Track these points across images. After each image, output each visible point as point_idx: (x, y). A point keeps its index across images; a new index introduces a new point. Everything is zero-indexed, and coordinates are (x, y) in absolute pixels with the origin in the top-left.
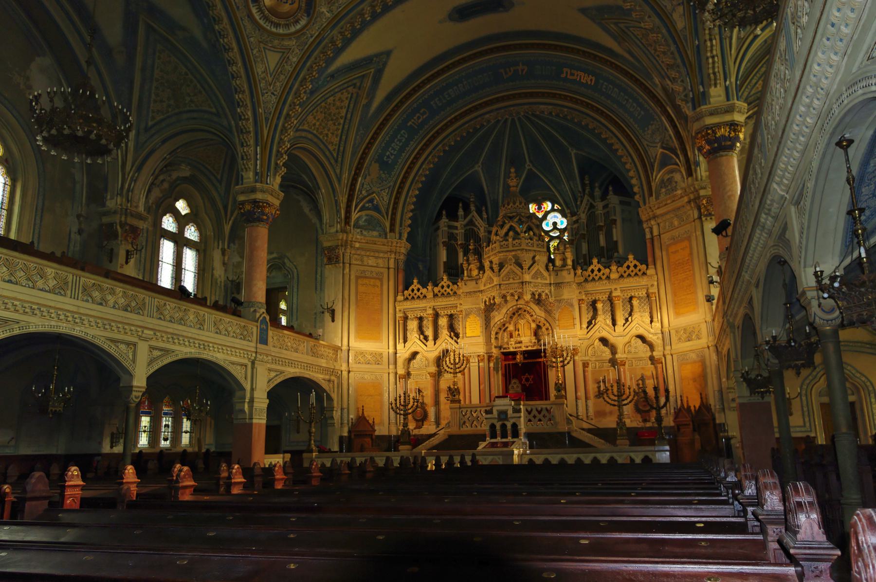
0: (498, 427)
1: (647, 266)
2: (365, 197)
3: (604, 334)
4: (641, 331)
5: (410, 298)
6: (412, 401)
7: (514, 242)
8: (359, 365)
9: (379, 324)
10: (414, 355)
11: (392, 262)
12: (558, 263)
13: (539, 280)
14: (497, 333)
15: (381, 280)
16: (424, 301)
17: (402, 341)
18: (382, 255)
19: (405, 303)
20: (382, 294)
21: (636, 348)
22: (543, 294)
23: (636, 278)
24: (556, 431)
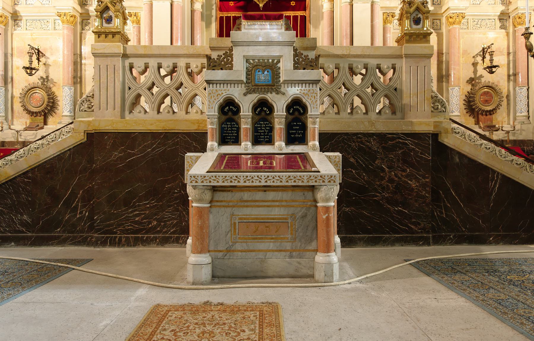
24: (406, 129)
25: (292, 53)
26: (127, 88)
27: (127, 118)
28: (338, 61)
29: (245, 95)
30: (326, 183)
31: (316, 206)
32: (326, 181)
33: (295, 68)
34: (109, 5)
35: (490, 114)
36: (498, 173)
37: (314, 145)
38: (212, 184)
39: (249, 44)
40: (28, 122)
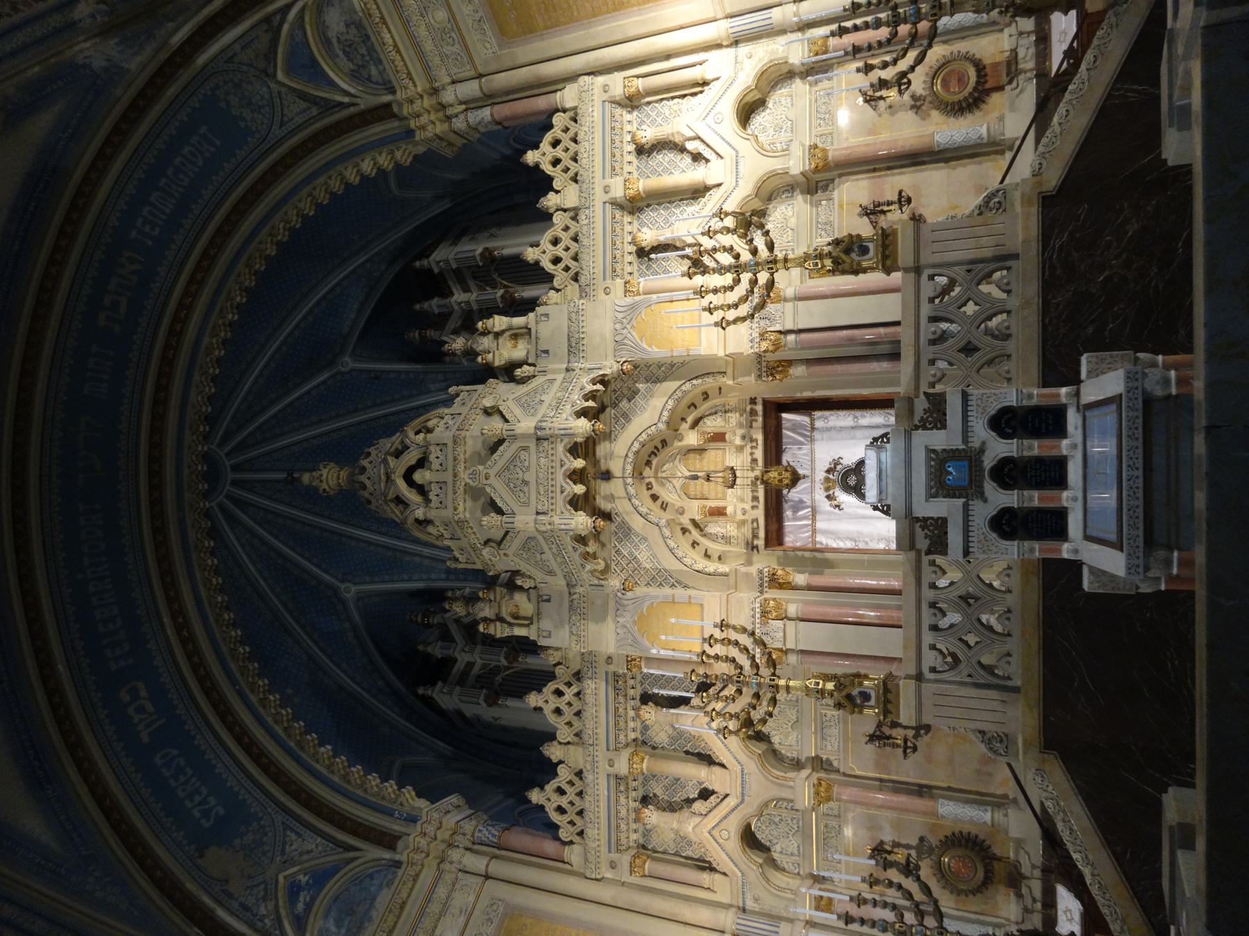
0: (1010, 499)
1: (557, 110)
2: (277, 906)
7: (435, 466)
14: (707, 556)
16: (589, 777)
17: (705, 878)
18: (441, 891)
22: (590, 387)
24: (1034, 249)
25: (920, 431)
26: (969, 680)
27: (1019, 683)
28: (924, 362)
29: (985, 501)
30: (1139, 384)
31: (1177, 396)
32: (1136, 384)
33: (944, 427)
34: (844, 693)
35: (984, 67)
36: (1112, 89)
37: (1068, 394)
38: (1141, 544)
40: (1002, 889)
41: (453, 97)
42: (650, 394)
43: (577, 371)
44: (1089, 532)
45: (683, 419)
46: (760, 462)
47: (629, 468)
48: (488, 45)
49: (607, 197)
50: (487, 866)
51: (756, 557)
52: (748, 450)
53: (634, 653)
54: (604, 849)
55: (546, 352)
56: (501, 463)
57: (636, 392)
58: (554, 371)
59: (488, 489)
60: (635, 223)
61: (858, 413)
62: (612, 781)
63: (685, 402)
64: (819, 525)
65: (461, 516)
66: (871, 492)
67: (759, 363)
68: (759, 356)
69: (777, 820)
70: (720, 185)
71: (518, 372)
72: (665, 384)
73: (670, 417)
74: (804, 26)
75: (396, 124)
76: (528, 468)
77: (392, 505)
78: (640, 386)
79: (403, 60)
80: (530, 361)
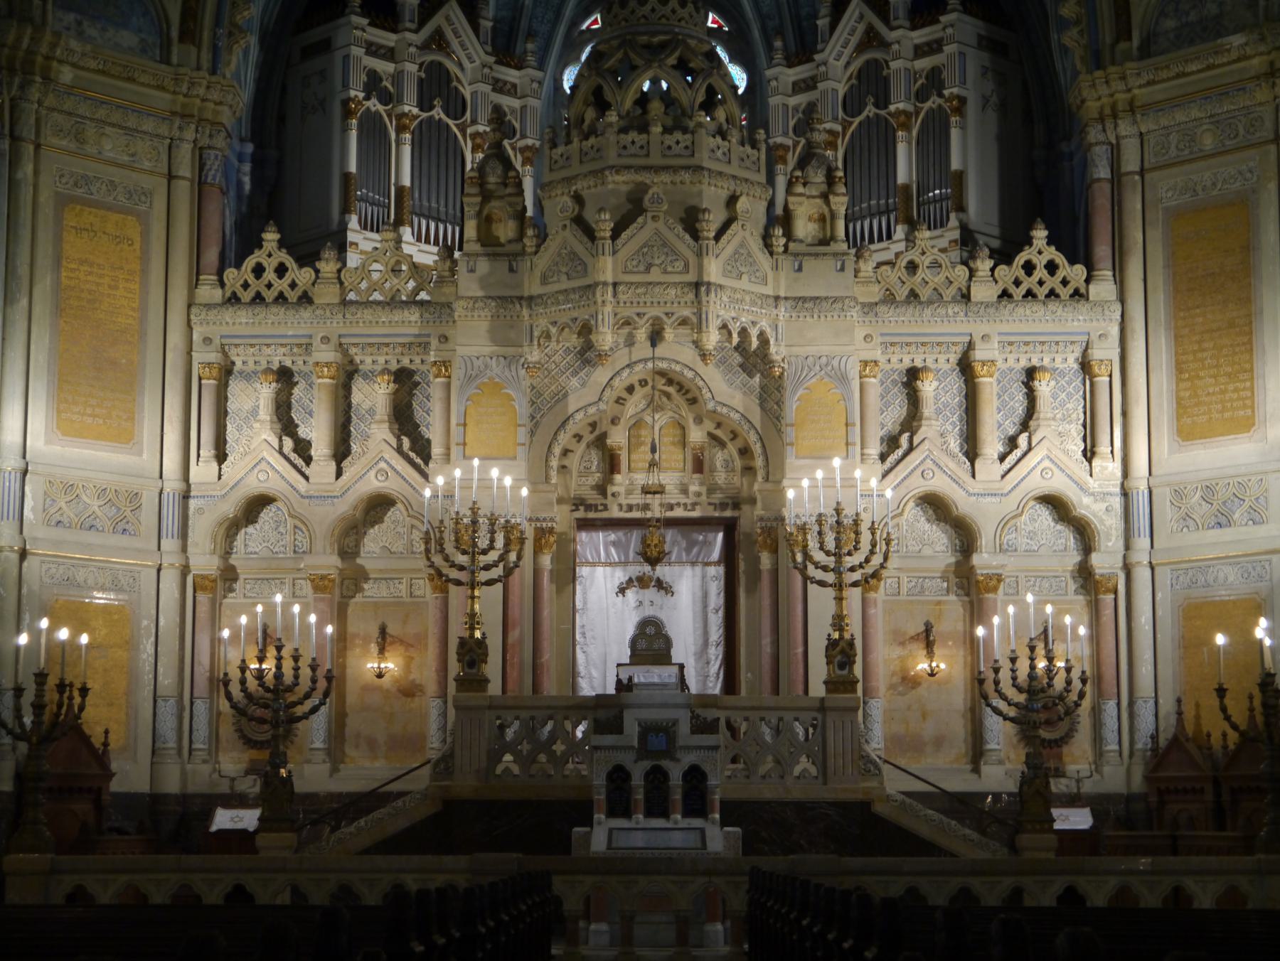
0: (637, 780)
1: (1090, 267)
3: (939, 484)
4: (1057, 484)
5: (246, 296)
6: (306, 672)
7: (669, 140)
8: (56, 533)
9: (129, 384)
10: (256, 505)
11: (185, 153)
12: (804, 228)
13: (744, 283)
14: (566, 452)
15: (144, 220)
16: (306, 313)
17: (208, 451)
18: (149, 125)
19: (228, 314)
20: (145, 272)
21: (1032, 535)
22: (754, 333)
23: (1053, 305)
33: (693, 732)
39: (640, 706)
41: (1124, 133)
42: (747, 391)
43: (775, 312)
44: (615, 832)
45: (719, 425)
46: (670, 514)
47: (663, 365)
48: (1170, 194)
49: (977, 339)
50: (184, 178)
51: (566, 508)
52: (683, 501)
53: (457, 373)
54: (225, 330)
55: (800, 269)
56: (670, 236)
57: (751, 375)
58: (776, 280)
59: (640, 220)
60: (949, 366)
61: (721, 613)
62: (304, 341)
63: (739, 429)
64: (600, 570)
65: (610, 178)
66: (642, 675)
67: (776, 519)
68: (783, 519)
69: (282, 529)
70: (974, 476)
71: (779, 231)
72: (758, 409)
73: (721, 415)
74: (1128, 569)
75: (1108, 40)
76: (665, 272)
77: (619, 55)
78: (757, 378)
79: (1169, 79)
80: (791, 245)
